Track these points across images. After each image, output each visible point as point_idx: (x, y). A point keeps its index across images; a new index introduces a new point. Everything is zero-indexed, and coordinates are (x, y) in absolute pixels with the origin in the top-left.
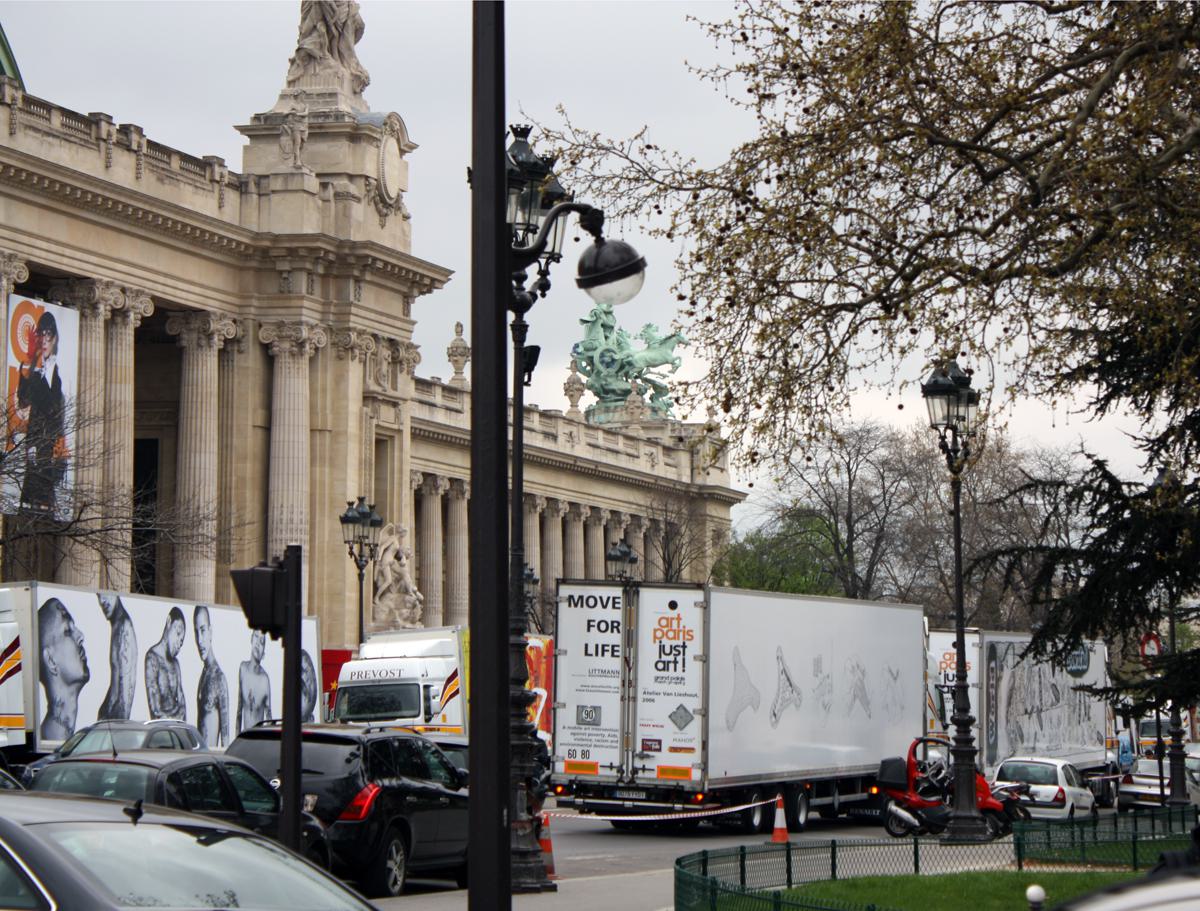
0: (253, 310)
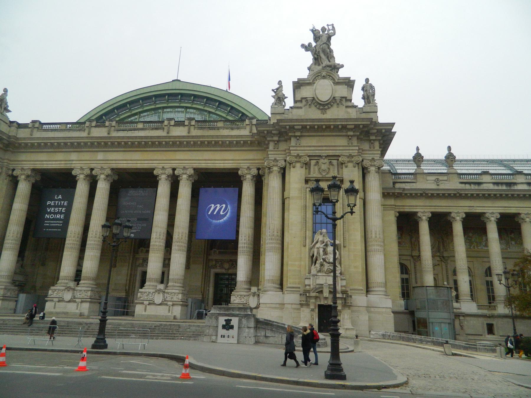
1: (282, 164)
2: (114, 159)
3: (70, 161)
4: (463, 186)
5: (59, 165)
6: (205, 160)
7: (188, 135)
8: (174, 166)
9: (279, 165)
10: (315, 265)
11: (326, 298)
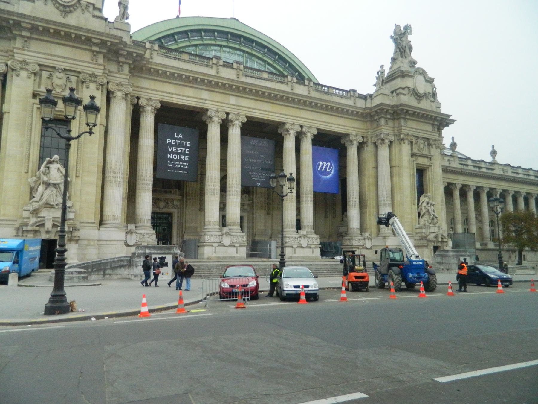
0: (369, 133)
1: (392, 138)
2: (246, 106)
3: (203, 99)
4: (460, 166)
5: (190, 102)
6: (325, 122)
7: (308, 95)
8: (302, 123)
9: (390, 139)
11: (439, 242)
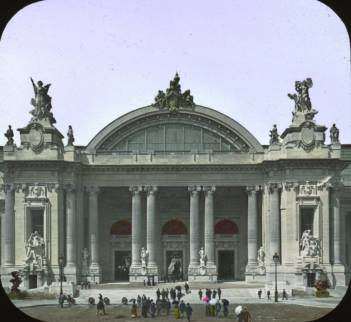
10: (303, 250)
